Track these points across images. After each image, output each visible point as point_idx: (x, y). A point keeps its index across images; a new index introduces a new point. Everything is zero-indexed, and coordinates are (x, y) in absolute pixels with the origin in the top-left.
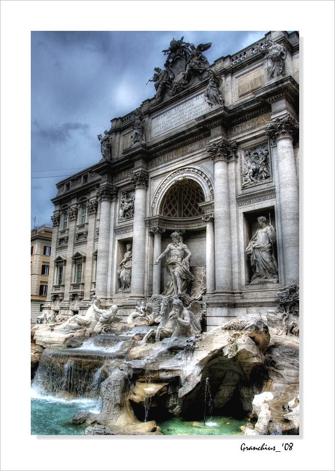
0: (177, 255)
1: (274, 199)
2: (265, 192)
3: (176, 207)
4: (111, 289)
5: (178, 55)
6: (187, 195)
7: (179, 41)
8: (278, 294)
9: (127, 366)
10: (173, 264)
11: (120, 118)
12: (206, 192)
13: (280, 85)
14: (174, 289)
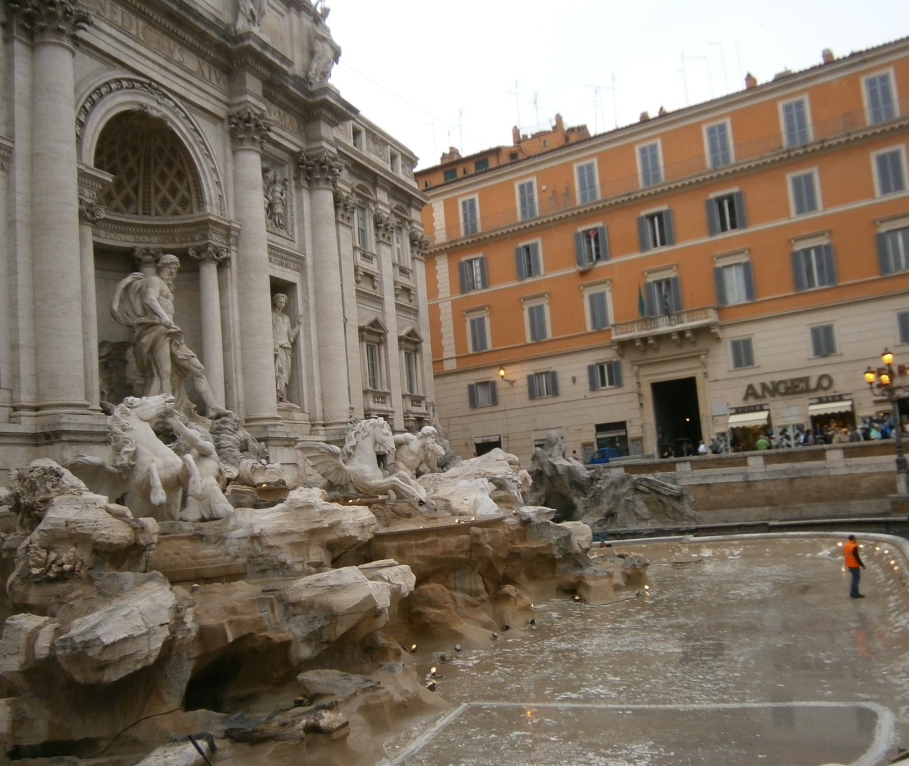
1: (297, 273)
12: (210, 191)
13: (349, 112)
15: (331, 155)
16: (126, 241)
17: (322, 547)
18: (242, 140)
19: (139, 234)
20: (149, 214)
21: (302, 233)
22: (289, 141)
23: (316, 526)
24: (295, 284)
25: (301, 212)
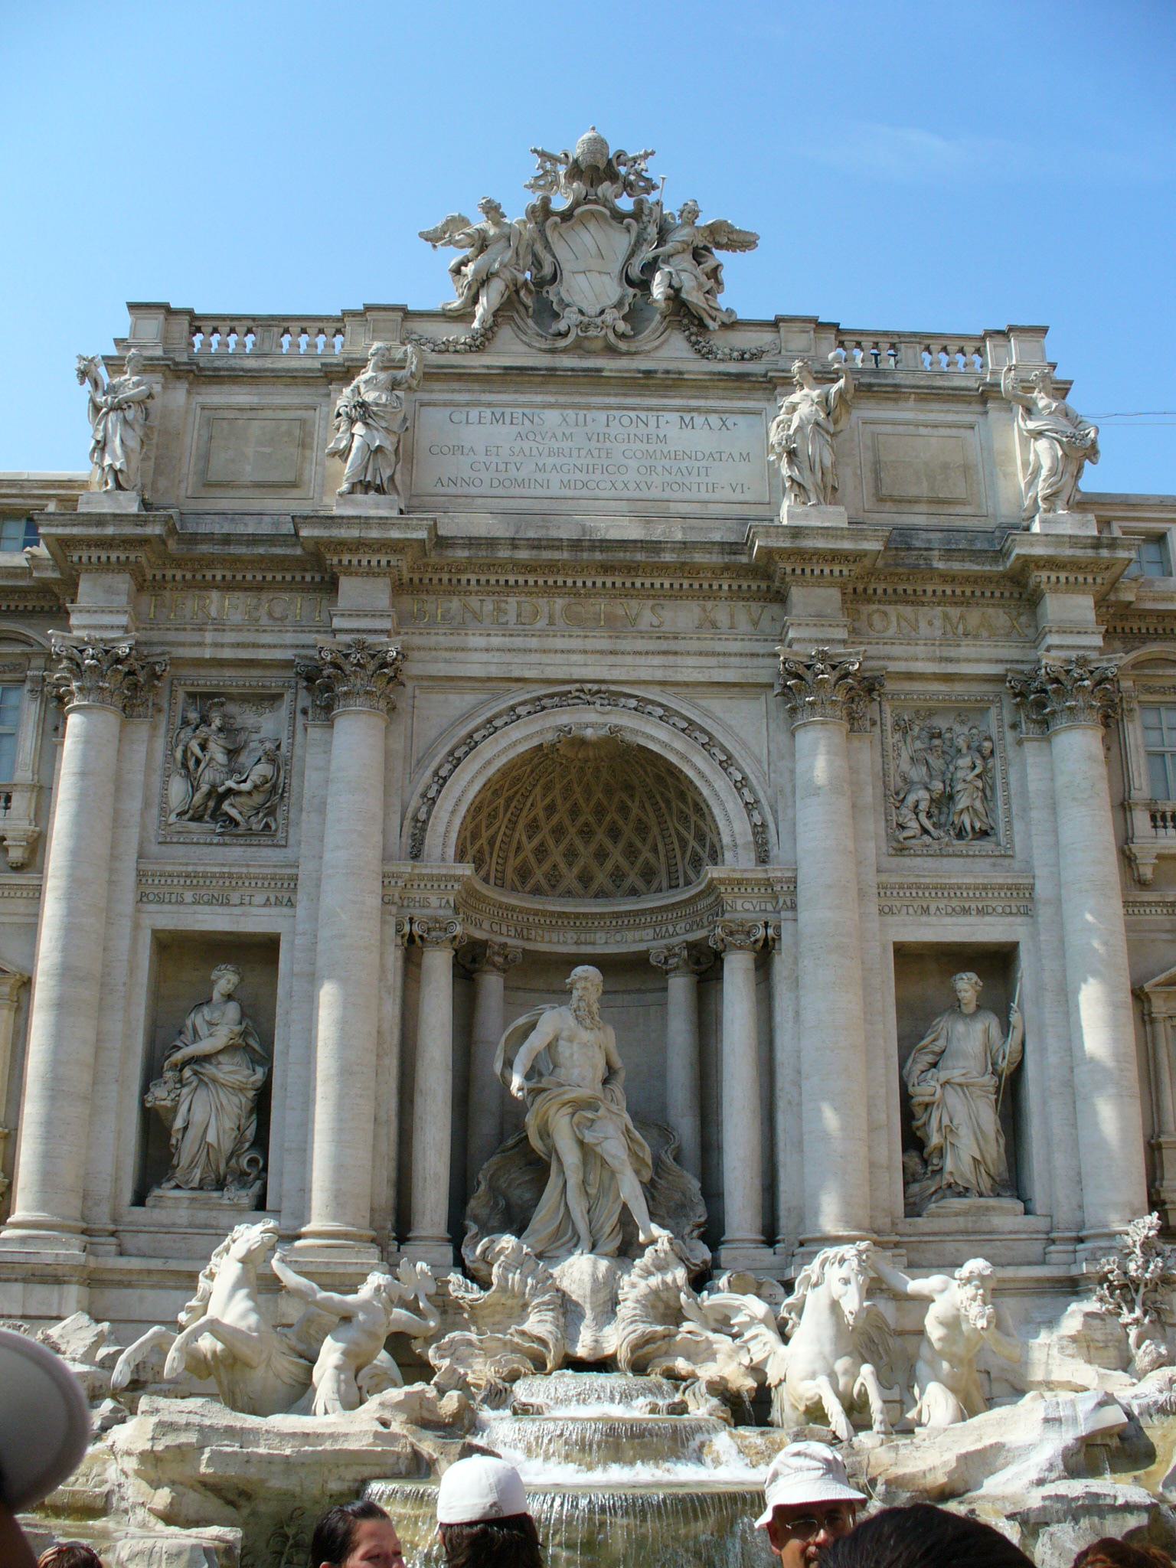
1: (1019, 920)
3: (491, 842)
4: (117, 1179)
5: (595, 202)
6: (548, 800)
7: (619, 155)
11: (190, 313)
12: (731, 822)
13: (1105, 553)
14: (566, 1205)
15: (1073, 655)
16: (641, 940)
17: (192, 1487)
18: (793, 710)
19: (660, 924)
20: (677, 886)
22: (978, 661)
23: (148, 1446)
25: (1024, 793)
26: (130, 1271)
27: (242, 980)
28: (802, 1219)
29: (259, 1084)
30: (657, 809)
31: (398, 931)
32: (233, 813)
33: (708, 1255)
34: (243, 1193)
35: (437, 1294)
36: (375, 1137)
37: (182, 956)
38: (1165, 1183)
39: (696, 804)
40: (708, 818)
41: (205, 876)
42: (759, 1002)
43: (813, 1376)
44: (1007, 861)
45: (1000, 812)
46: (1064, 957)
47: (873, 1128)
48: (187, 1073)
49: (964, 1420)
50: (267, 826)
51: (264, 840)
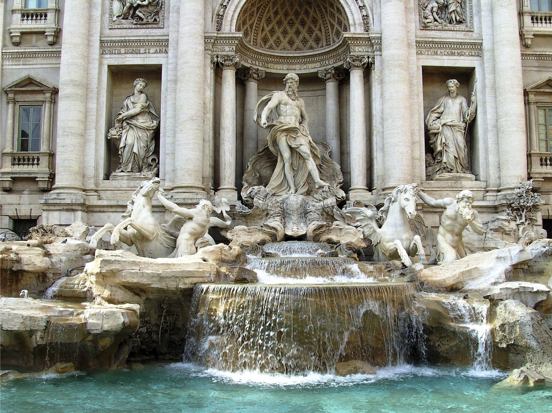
0: (296, 117)
1: (475, 58)
2: (464, 44)
4: (96, 169)
6: (274, 10)
8: (505, 195)
9: (510, 292)
10: (291, 131)
12: (353, 15)
14: (285, 174)
16: (315, 68)
19: (323, 60)
21: (480, 23)
23: (99, 270)
24: (473, 69)
26: (103, 206)
27: (146, 85)
28: (383, 180)
29: (155, 128)
30: (321, 12)
31: (211, 61)
32: (141, 15)
33: (344, 195)
34: (149, 173)
35: (230, 211)
36: (204, 147)
37: (121, 75)
38: (532, 170)
39: (338, 9)
40: (343, 14)
41: (129, 41)
42: (365, 91)
43: (392, 240)
44: (470, 33)
45: (468, 13)
46: (494, 73)
47: (413, 143)
48: (125, 124)
49: (458, 259)
50: (155, 20)
51: (154, 26)
